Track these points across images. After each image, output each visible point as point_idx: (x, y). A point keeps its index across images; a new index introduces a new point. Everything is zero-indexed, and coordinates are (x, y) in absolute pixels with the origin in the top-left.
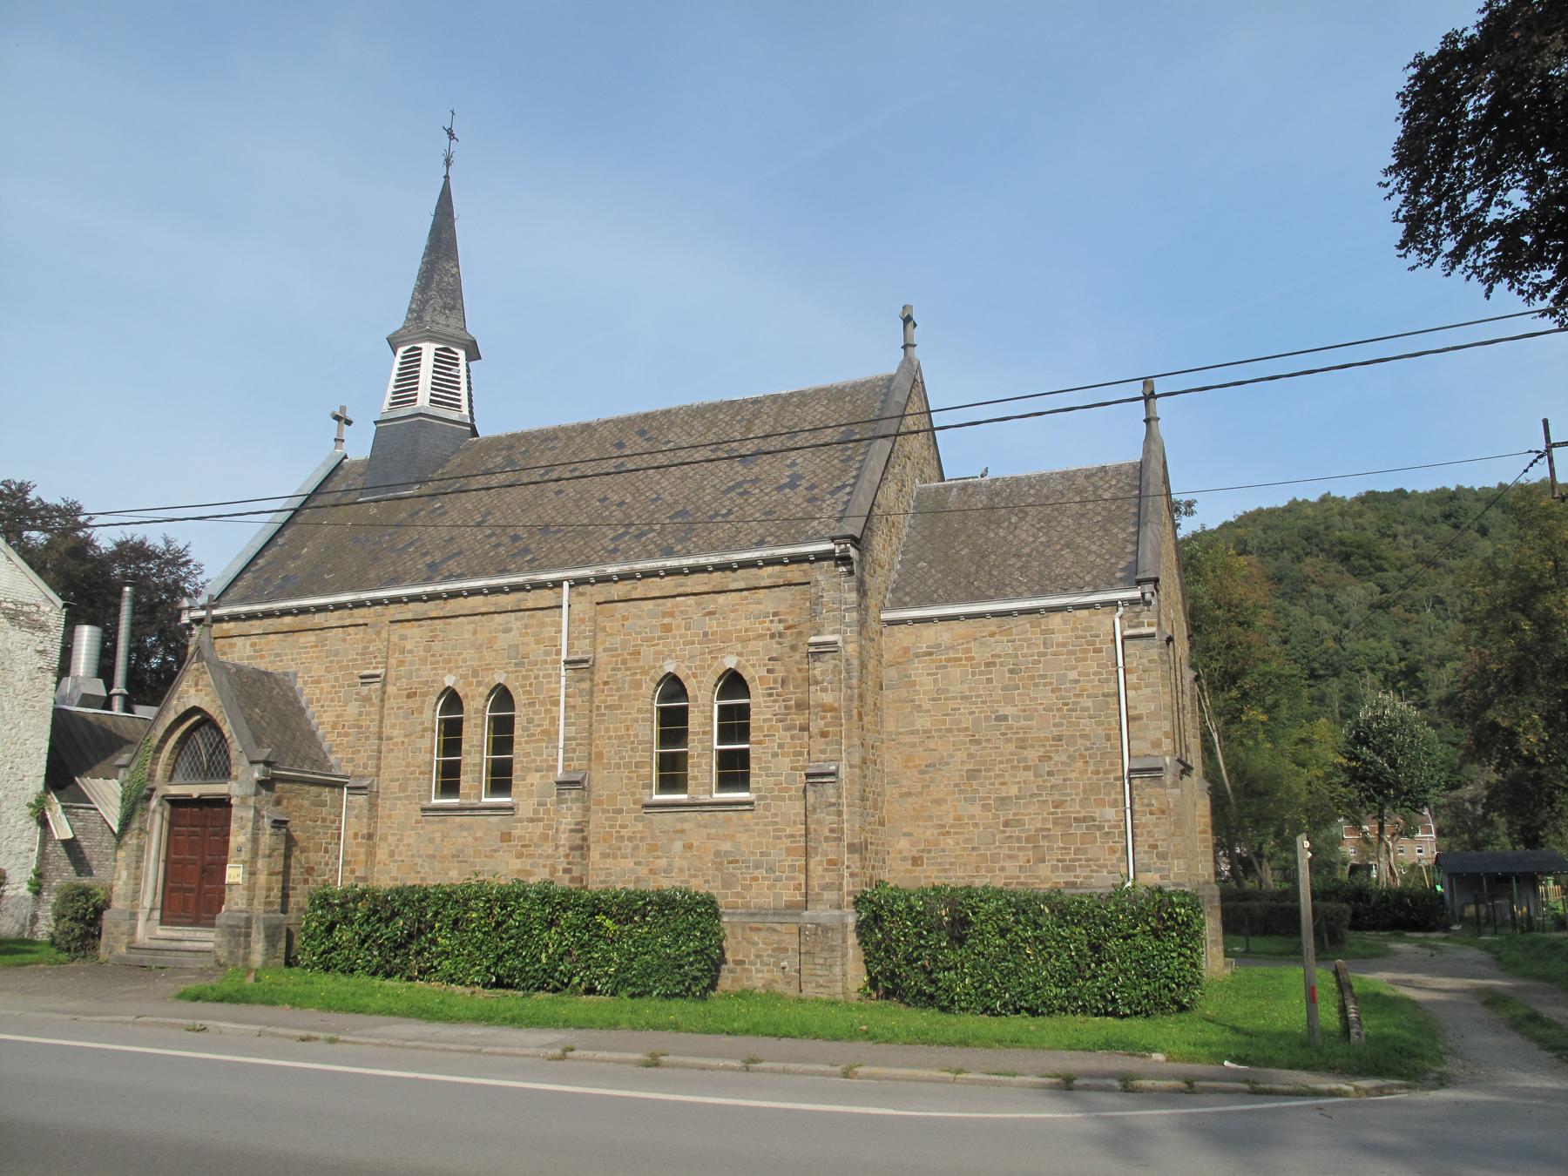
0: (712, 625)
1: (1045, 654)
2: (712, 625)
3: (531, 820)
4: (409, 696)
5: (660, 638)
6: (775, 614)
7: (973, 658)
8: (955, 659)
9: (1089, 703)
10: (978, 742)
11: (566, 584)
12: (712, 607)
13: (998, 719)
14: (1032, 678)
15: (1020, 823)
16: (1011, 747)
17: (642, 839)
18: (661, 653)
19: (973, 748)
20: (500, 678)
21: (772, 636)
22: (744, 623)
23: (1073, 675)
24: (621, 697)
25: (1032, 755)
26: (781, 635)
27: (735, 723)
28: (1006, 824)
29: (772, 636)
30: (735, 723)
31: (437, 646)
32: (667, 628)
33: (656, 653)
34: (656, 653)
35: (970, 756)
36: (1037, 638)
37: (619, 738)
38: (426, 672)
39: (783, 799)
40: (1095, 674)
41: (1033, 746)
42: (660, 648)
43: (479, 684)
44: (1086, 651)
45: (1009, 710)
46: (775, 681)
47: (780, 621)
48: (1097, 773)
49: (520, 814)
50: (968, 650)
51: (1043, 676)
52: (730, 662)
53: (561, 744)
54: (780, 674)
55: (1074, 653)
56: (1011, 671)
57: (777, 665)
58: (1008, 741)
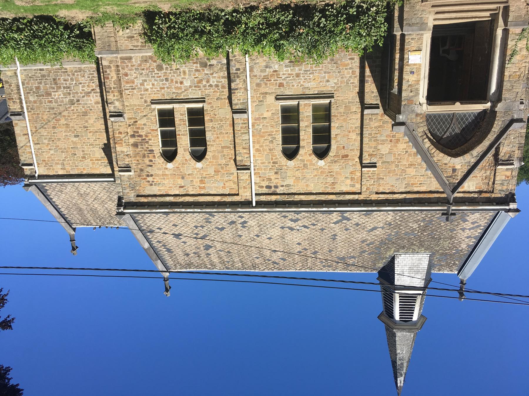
0: (181, 182)
1: (63, 160)
2: (181, 182)
3: (266, 93)
4: (347, 156)
5: (205, 178)
6: (151, 185)
7: (91, 160)
8: (97, 160)
9: (46, 141)
10: (85, 127)
11: (254, 204)
12: (182, 189)
13: (78, 136)
14: (67, 152)
15: (64, 94)
16: (71, 125)
17: (205, 86)
18: (204, 171)
19: (86, 125)
20: (291, 163)
21: (152, 175)
22: (166, 182)
23: (52, 152)
24: (223, 152)
25: (63, 121)
26: (148, 176)
27: (169, 139)
28: (69, 94)
29: (152, 175)
30: (169, 139)
31: (330, 180)
32: (202, 182)
33: (207, 171)
34: (207, 171)
35: (87, 122)
36: (68, 168)
37: (221, 133)
38: (336, 167)
39: (139, 105)
40: (44, 152)
41: (64, 125)
42: (205, 173)
43: (303, 161)
44: (48, 161)
45: (75, 139)
46: (148, 157)
47: (149, 182)
48: (38, 114)
49: (273, 97)
50: (93, 163)
51: (62, 152)
52: (170, 165)
53: (251, 131)
54: (147, 161)
55: (52, 160)
56: (75, 154)
57: (148, 163)
58: (72, 127)
